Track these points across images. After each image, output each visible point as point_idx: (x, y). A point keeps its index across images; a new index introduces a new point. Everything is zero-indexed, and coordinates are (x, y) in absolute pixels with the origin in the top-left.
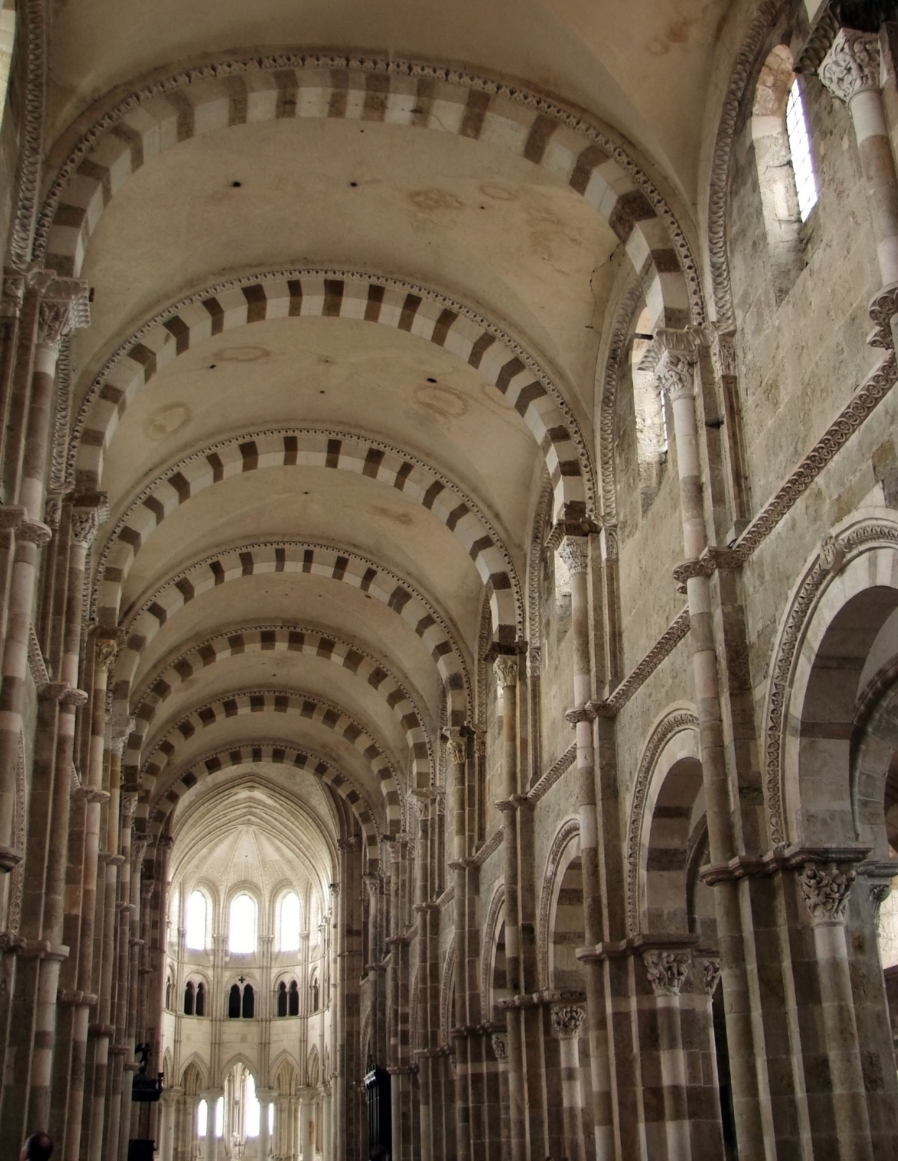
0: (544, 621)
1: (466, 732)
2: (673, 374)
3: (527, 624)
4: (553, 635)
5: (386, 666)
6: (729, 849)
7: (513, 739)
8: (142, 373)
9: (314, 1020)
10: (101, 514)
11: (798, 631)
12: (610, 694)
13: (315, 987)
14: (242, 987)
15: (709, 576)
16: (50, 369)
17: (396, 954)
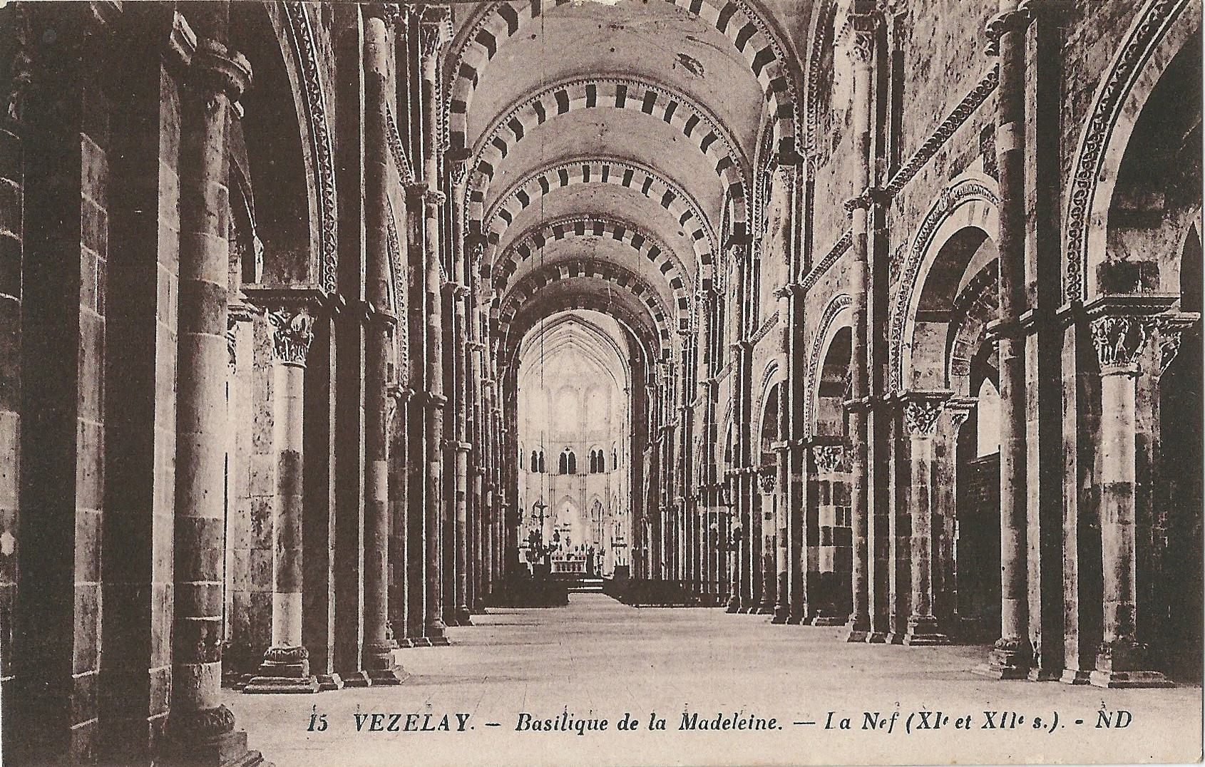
0: (764, 220)
1: (712, 294)
2: (858, 50)
3: (753, 222)
4: (770, 232)
5: (659, 245)
6: (863, 391)
7: (740, 302)
8: (485, 50)
9: (614, 474)
10: (469, 163)
11: (921, 251)
12: (803, 279)
13: (615, 454)
14: (567, 453)
15: (867, 209)
16: (431, 77)
17: (666, 438)
